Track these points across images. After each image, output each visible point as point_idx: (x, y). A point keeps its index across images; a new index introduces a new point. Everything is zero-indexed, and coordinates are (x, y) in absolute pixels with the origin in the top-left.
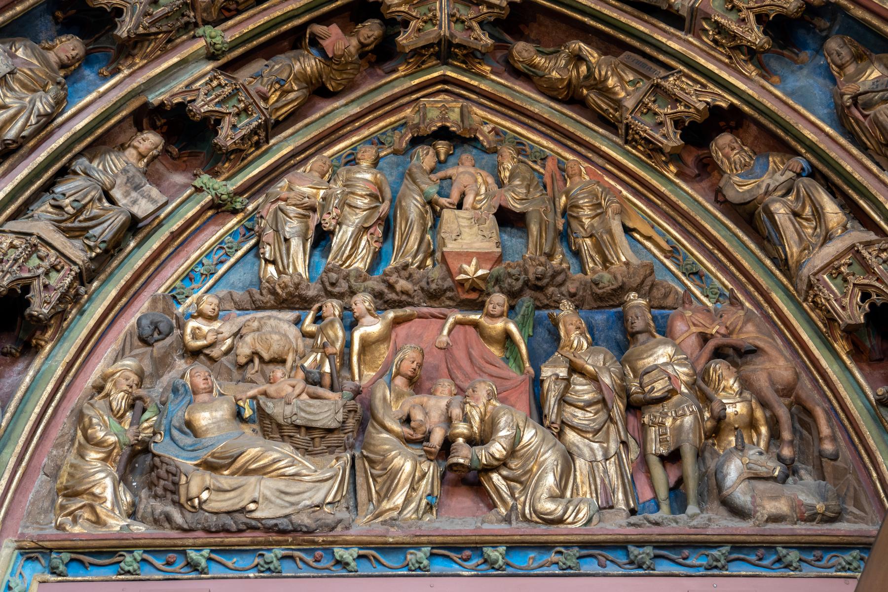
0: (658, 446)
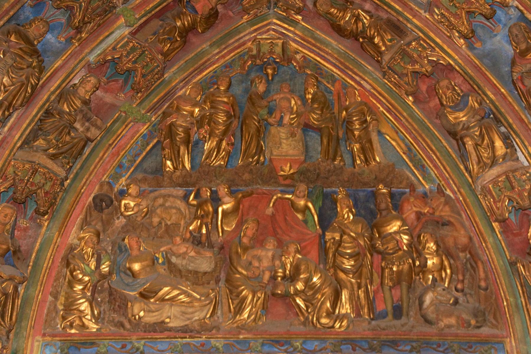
0: (389, 281)
